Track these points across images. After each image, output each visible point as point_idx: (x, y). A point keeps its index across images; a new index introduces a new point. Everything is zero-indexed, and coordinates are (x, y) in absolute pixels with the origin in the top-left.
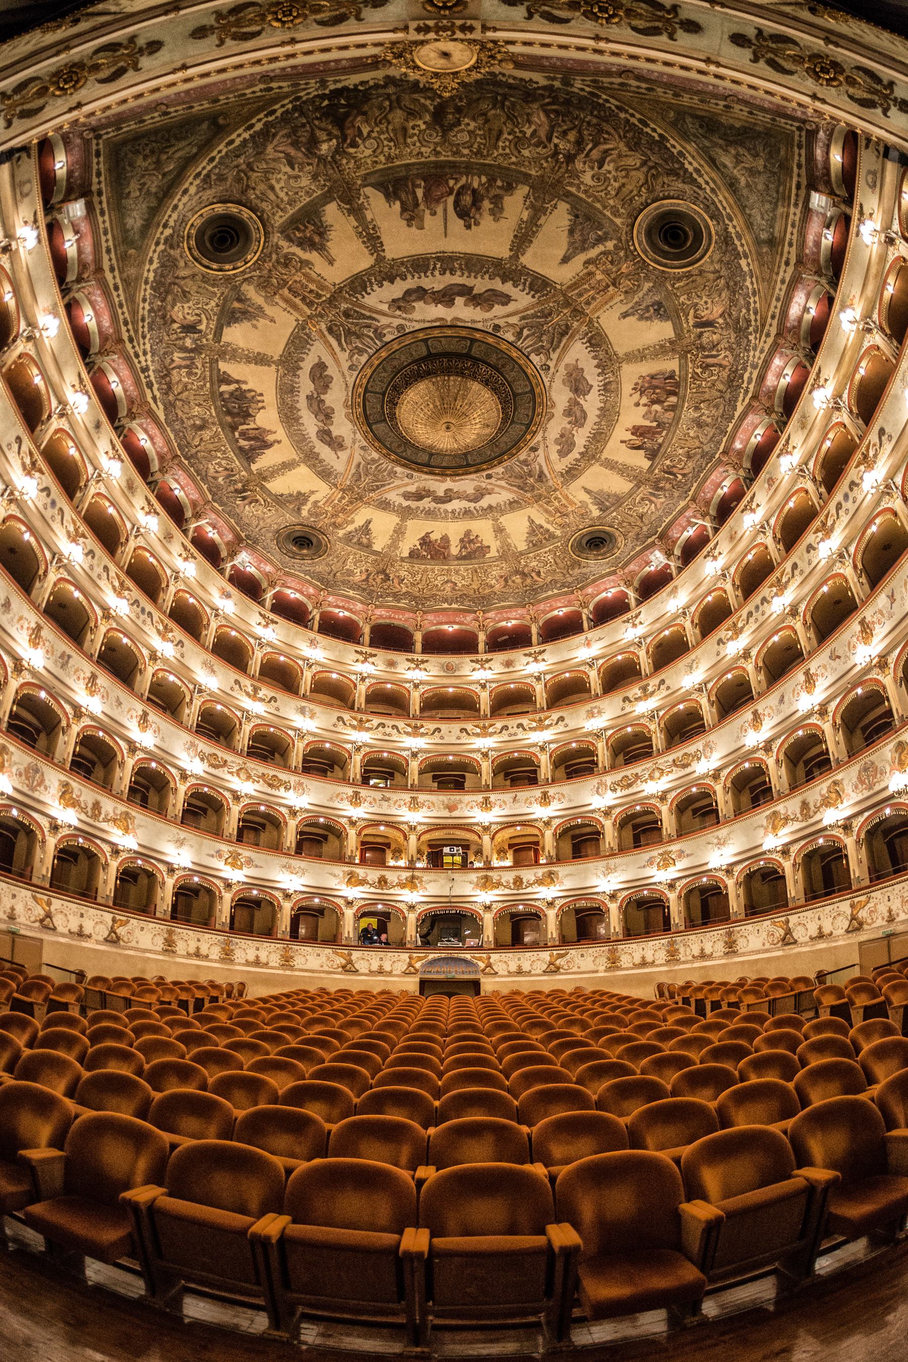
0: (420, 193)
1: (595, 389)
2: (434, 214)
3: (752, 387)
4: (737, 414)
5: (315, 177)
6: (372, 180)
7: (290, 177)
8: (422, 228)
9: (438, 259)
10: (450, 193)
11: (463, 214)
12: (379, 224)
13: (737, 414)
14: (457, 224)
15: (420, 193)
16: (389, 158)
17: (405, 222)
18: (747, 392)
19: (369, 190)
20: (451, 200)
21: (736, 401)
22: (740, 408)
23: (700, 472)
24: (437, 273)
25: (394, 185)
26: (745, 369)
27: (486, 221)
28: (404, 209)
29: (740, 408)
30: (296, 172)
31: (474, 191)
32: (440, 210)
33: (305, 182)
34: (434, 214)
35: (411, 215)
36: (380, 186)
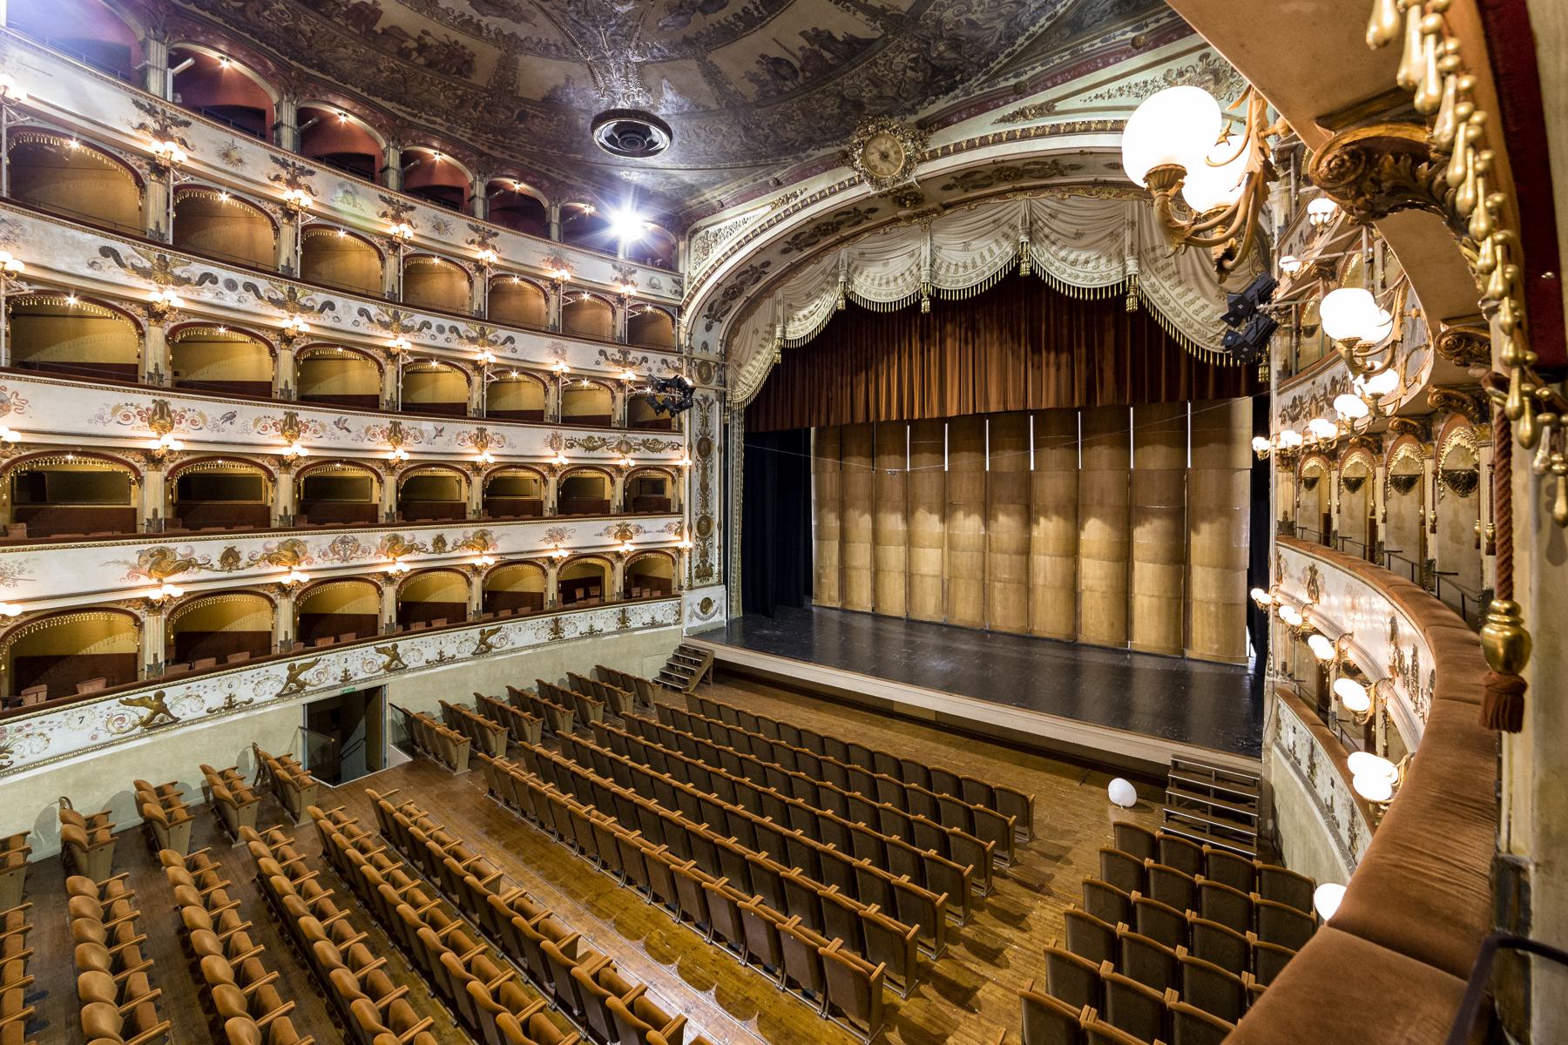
0: (827, 55)
1: (477, 16)
2: (801, 49)
3: (423, 122)
4: (378, 100)
5: (939, 23)
6: (878, 45)
7: (969, 10)
8: (803, 34)
9: (763, 19)
10: (803, 69)
11: (777, 61)
12: (846, 15)
13: (378, 100)
14: (775, 52)
15: (827, 55)
16: (876, 64)
17: (821, 28)
18: (415, 116)
19: (877, 35)
20: (797, 64)
21: (399, 102)
22: (387, 105)
23: (253, 34)
24: (751, 7)
25: (855, 48)
26: (448, 120)
27: (754, 68)
28: (831, 37)
29: (387, 105)
30: (962, 18)
31: (785, 79)
32: (799, 54)
33: (948, 14)
34: (801, 49)
35: (821, 38)
36: (869, 42)
